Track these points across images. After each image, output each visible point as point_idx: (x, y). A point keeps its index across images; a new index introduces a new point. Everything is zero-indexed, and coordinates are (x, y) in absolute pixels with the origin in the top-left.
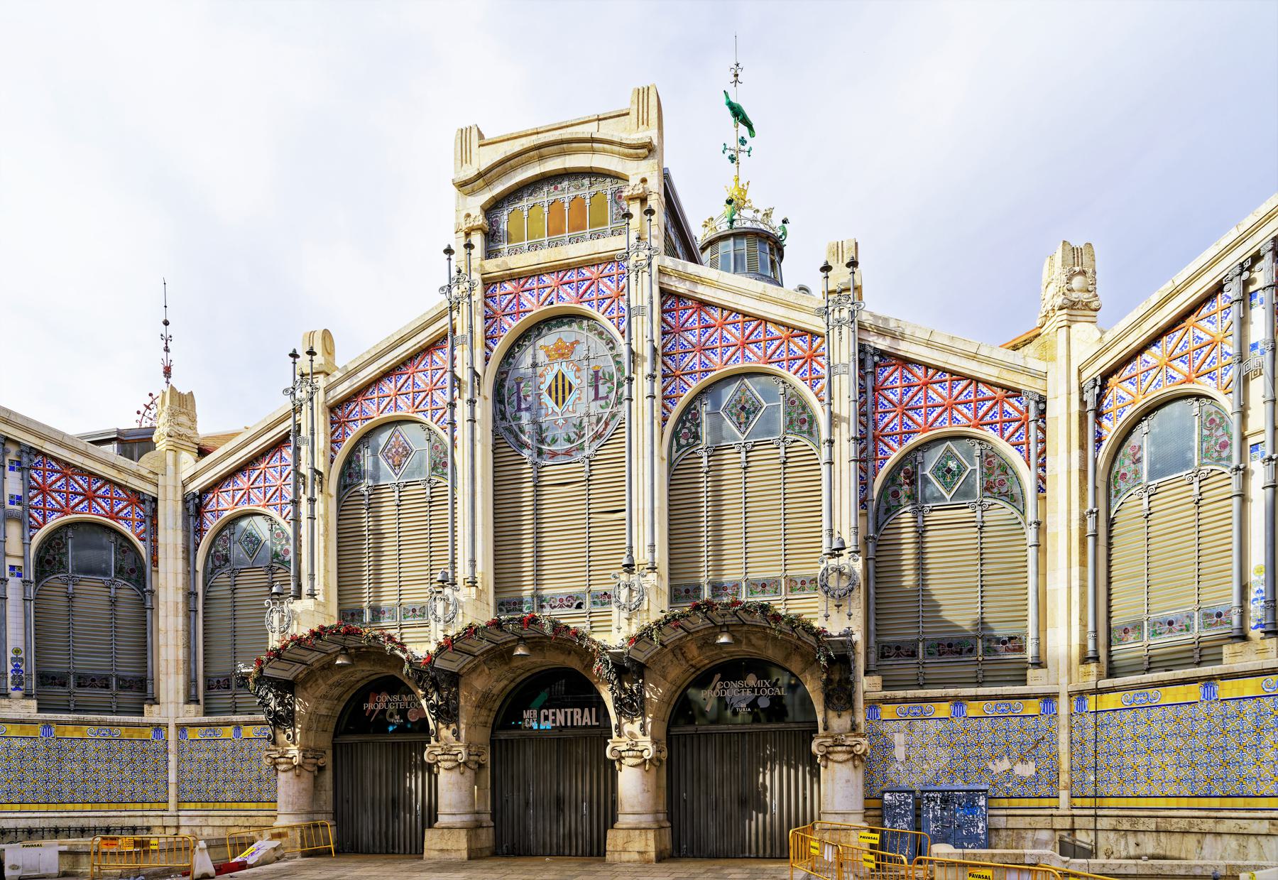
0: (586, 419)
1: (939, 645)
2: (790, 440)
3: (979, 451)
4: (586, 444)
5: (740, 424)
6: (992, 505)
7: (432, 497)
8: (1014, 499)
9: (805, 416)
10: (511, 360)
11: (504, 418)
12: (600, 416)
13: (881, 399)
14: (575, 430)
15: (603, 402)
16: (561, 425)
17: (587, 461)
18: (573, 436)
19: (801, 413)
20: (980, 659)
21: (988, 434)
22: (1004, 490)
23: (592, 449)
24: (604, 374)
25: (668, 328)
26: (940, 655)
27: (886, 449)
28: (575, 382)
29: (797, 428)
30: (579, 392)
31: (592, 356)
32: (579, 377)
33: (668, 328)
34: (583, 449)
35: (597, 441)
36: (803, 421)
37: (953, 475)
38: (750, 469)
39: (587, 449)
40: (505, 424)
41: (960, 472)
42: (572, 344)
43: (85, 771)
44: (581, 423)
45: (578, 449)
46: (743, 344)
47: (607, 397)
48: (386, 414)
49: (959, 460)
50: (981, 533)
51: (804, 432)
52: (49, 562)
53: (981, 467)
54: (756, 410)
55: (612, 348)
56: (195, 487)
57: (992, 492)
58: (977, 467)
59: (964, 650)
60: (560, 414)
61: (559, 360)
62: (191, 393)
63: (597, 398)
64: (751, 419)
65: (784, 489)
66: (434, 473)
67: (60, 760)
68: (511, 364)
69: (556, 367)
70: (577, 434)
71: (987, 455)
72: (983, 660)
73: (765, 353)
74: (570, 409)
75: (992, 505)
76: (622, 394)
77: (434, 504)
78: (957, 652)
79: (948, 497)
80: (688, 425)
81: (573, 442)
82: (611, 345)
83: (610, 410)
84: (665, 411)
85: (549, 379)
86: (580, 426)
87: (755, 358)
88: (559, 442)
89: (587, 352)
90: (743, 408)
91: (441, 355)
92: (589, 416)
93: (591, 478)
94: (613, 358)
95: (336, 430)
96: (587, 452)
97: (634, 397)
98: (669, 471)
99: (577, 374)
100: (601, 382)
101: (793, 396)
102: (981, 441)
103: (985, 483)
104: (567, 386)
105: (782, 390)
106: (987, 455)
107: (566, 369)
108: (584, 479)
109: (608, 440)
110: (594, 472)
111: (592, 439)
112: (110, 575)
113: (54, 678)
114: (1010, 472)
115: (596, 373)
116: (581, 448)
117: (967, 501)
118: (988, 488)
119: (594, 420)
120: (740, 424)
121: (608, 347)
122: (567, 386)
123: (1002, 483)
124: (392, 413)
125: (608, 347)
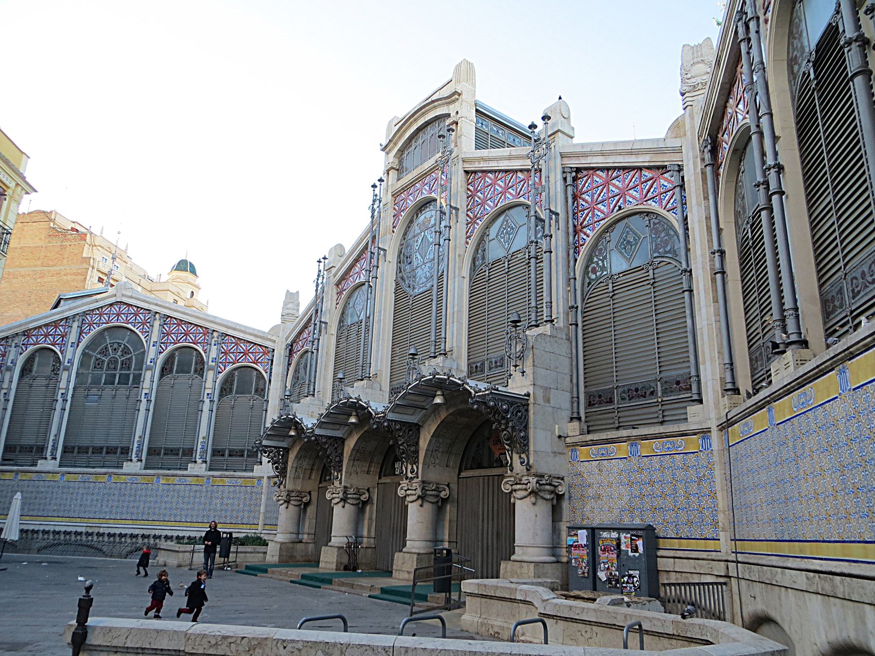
1: (629, 390)
6: (660, 262)
11: (401, 272)
20: (660, 400)
22: (668, 249)
26: (630, 400)
40: (400, 275)
43: (222, 504)
52: (225, 390)
56: (289, 341)
59: (648, 393)
62: (298, 292)
67: (211, 498)
72: (662, 401)
75: (660, 262)
78: (642, 396)
98: (470, 283)
112: (250, 393)
113: (219, 452)
123: (666, 243)
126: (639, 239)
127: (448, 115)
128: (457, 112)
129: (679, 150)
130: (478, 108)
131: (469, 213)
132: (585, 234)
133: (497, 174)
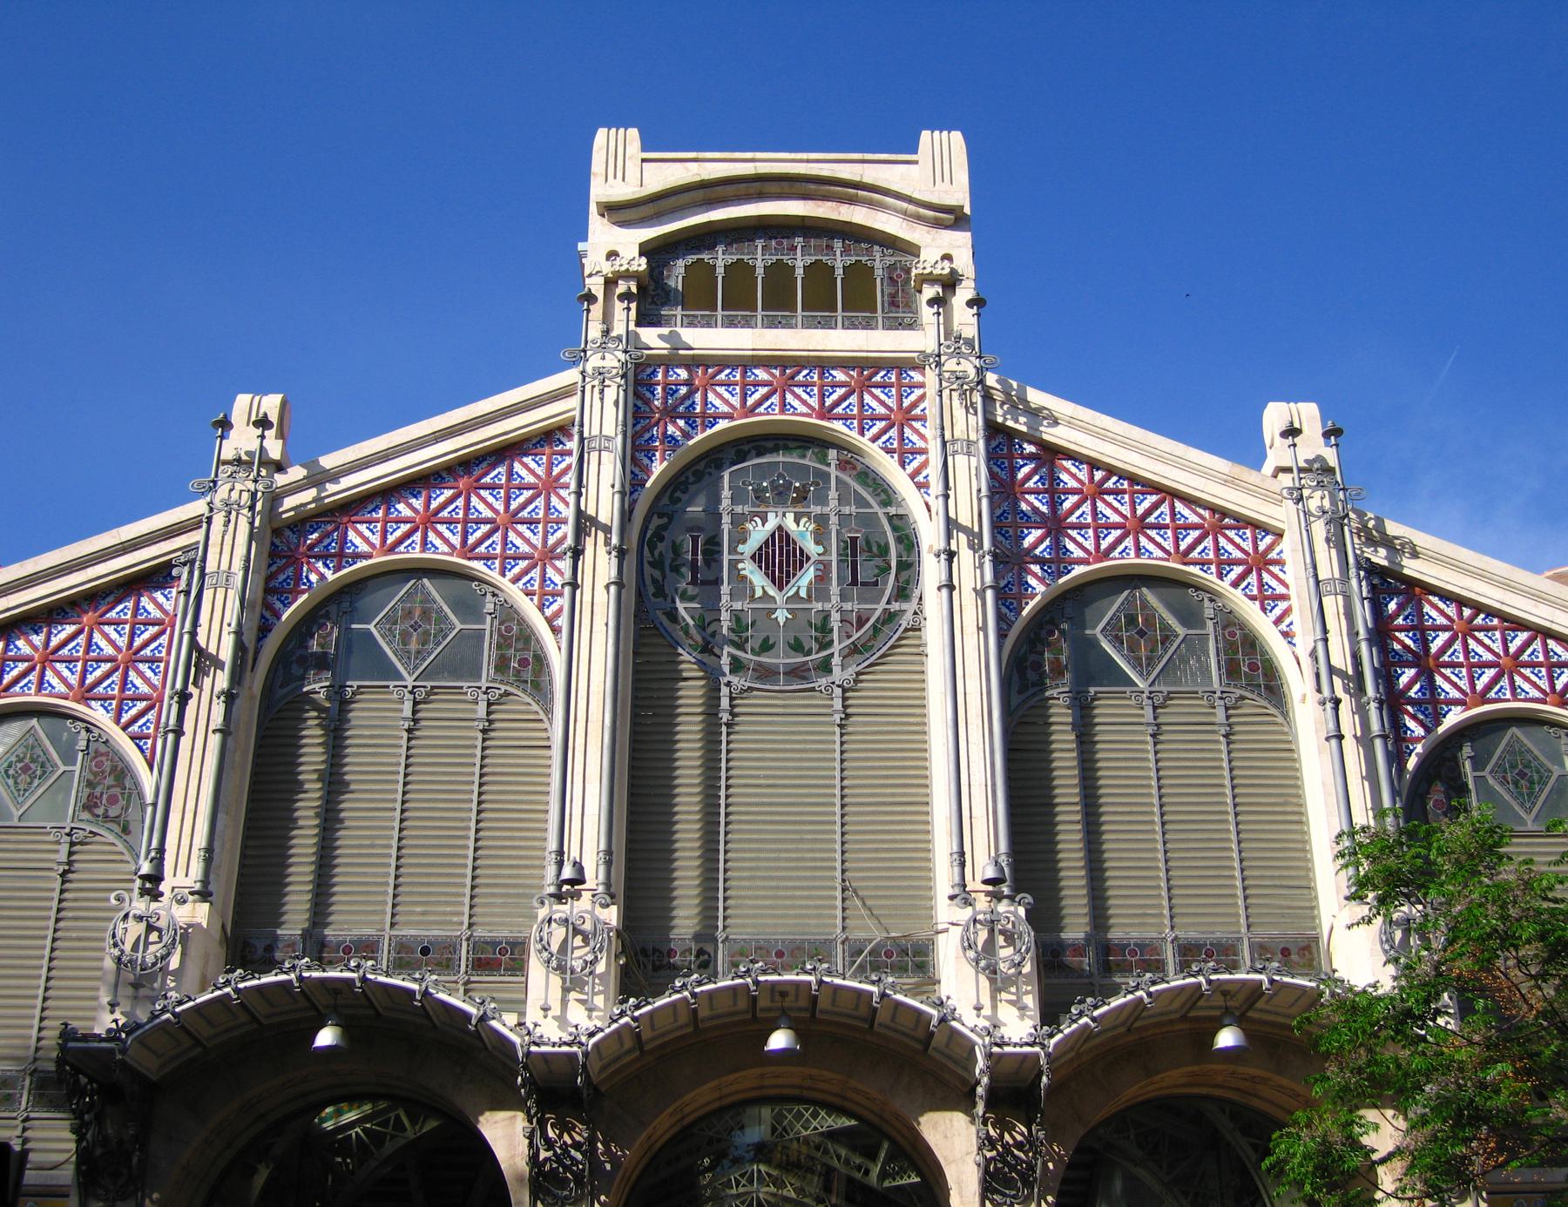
0: (835, 617)
4: (836, 660)
10: (678, 494)
16: (781, 621)
17: (838, 691)
24: (868, 543)
28: (812, 549)
34: (830, 671)
39: (836, 670)
44: (826, 617)
48: (402, 554)
55: (886, 503)
63: (854, 582)
68: (679, 500)
69: (772, 522)
74: (803, 593)
76: (908, 582)
81: (809, 653)
82: (883, 496)
83: (882, 605)
85: (758, 533)
86: (824, 627)
87: (1158, 553)
91: (533, 465)
94: (890, 518)
95: (281, 570)
97: (956, 582)
111: (847, 650)
116: (825, 667)
121: (879, 499)
124: (416, 554)
133: (1098, 475)
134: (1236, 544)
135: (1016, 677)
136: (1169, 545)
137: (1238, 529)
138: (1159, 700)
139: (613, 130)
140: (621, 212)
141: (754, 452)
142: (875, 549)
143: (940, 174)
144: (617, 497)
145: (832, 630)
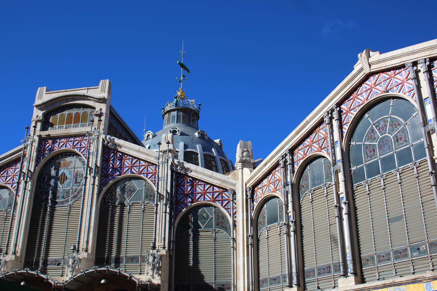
0: (71, 190)
2: (146, 203)
3: (214, 210)
4: (70, 200)
5: (128, 195)
7: (7, 217)
8: (227, 229)
9: (152, 194)
10: (46, 167)
12: (76, 189)
13: (180, 190)
14: (66, 194)
15: (78, 184)
16: (61, 192)
17: (69, 206)
18: (65, 196)
19: (151, 193)
21: (218, 205)
23: (72, 202)
24: (80, 174)
25: (105, 159)
27: (180, 208)
28: (69, 176)
29: (149, 198)
30: (69, 180)
31: (76, 167)
32: (70, 175)
33: (105, 159)
35: (74, 199)
36: (151, 196)
37: (205, 219)
38: (130, 213)
41: (207, 218)
42: (70, 162)
44: (69, 191)
45: (66, 201)
46: (131, 167)
47: (80, 183)
49: (207, 213)
50: (215, 241)
51: (151, 200)
53: (215, 216)
54: (134, 191)
57: (219, 226)
58: (214, 216)
60: (61, 188)
61: (64, 168)
63: (76, 183)
64: (132, 194)
65: (143, 221)
66: (9, 207)
70: (67, 196)
71: (217, 212)
73: (139, 170)
74: (66, 186)
77: (7, 220)
79: (203, 227)
80: (109, 195)
81: (65, 199)
82: (84, 164)
84: (100, 189)
88: (59, 198)
89: (74, 166)
90: (130, 190)
92: (72, 189)
93: (70, 213)
96: (70, 203)
99: (70, 173)
100: (78, 177)
101: (148, 186)
102: (215, 207)
103: (216, 222)
104: (65, 178)
105: (144, 184)
106: (217, 212)
107: (66, 171)
108: (67, 213)
109: (78, 199)
110: (71, 211)
114: (225, 219)
115: (77, 173)
116: (67, 201)
117: (210, 229)
118: (217, 224)
119: (74, 190)
120: (128, 195)
121: (83, 164)
122: (65, 178)
125: (83, 164)
126: (209, 217)
127: (94, 108)
128: (101, 109)
129: (235, 185)
130: (111, 109)
131: (103, 170)
132: (181, 206)
134: (151, 169)
135: (103, 201)
136: (137, 170)
137: (152, 165)
138: (131, 204)
139: (42, 87)
140: (40, 107)
141: (61, 156)
142: (81, 175)
143: (103, 90)
144: (27, 170)
145: (70, 193)
